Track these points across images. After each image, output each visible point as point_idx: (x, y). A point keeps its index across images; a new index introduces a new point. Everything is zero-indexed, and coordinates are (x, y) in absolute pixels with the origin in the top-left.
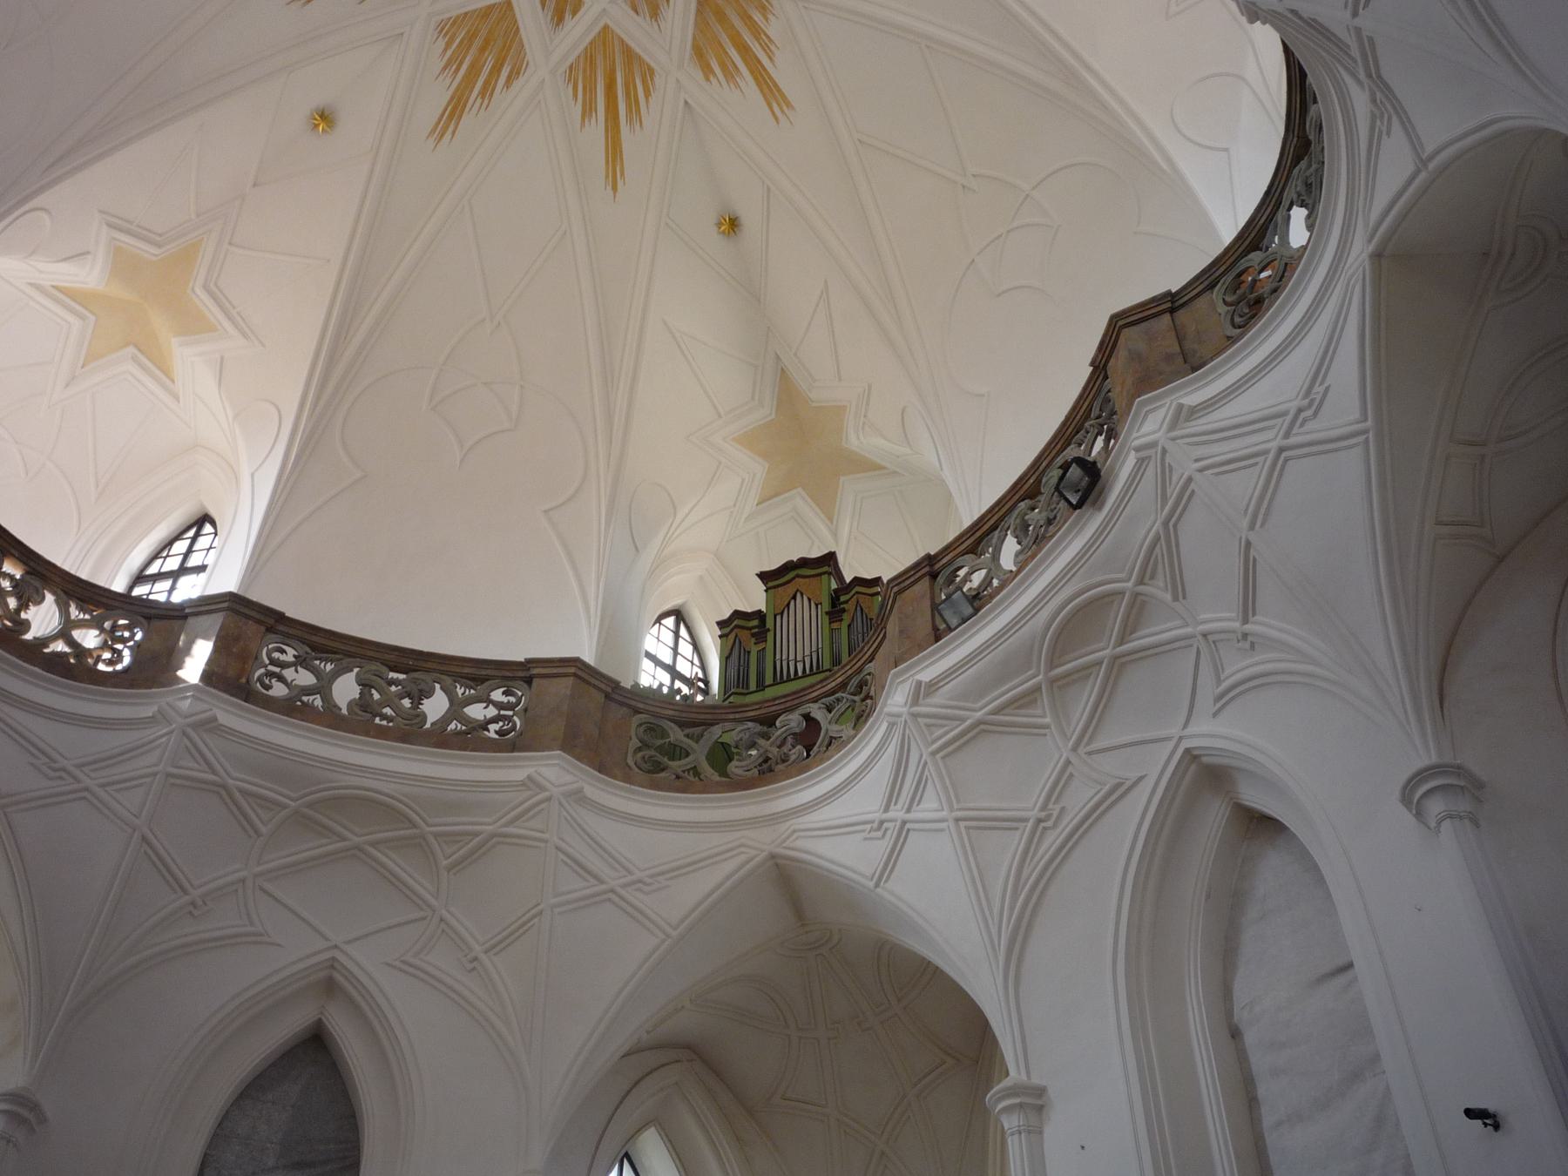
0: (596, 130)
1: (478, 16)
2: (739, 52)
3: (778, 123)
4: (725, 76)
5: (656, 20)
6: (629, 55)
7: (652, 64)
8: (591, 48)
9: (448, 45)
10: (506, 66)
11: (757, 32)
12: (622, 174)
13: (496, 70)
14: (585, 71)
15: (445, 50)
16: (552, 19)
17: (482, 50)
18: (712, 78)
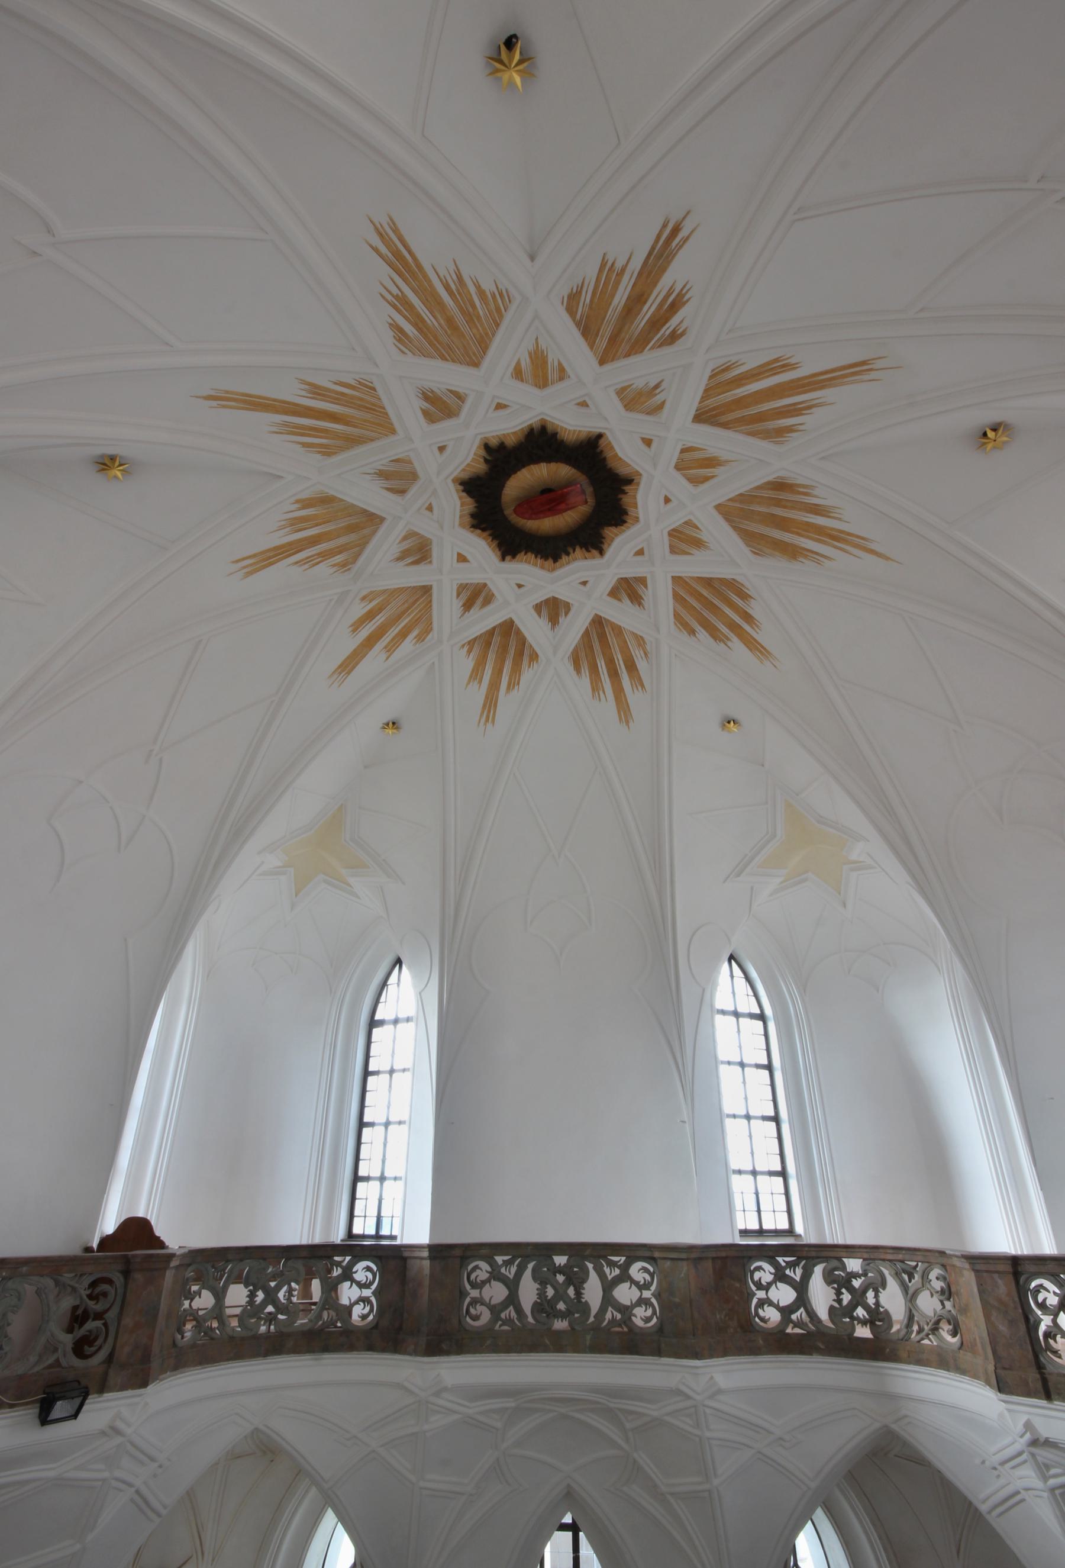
0: (291, 392)
1: (487, 334)
2: (312, 536)
3: (233, 562)
4: (295, 518)
5: (375, 473)
6: (353, 442)
7: (335, 459)
8: (380, 412)
9: (481, 293)
10: (416, 332)
11: (325, 555)
12: (224, 407)
13: (418, 323)
14: (361, 399)
15: (478, 287)
16: (432, 392)
17: (450, 321)
18: (297, 506)
